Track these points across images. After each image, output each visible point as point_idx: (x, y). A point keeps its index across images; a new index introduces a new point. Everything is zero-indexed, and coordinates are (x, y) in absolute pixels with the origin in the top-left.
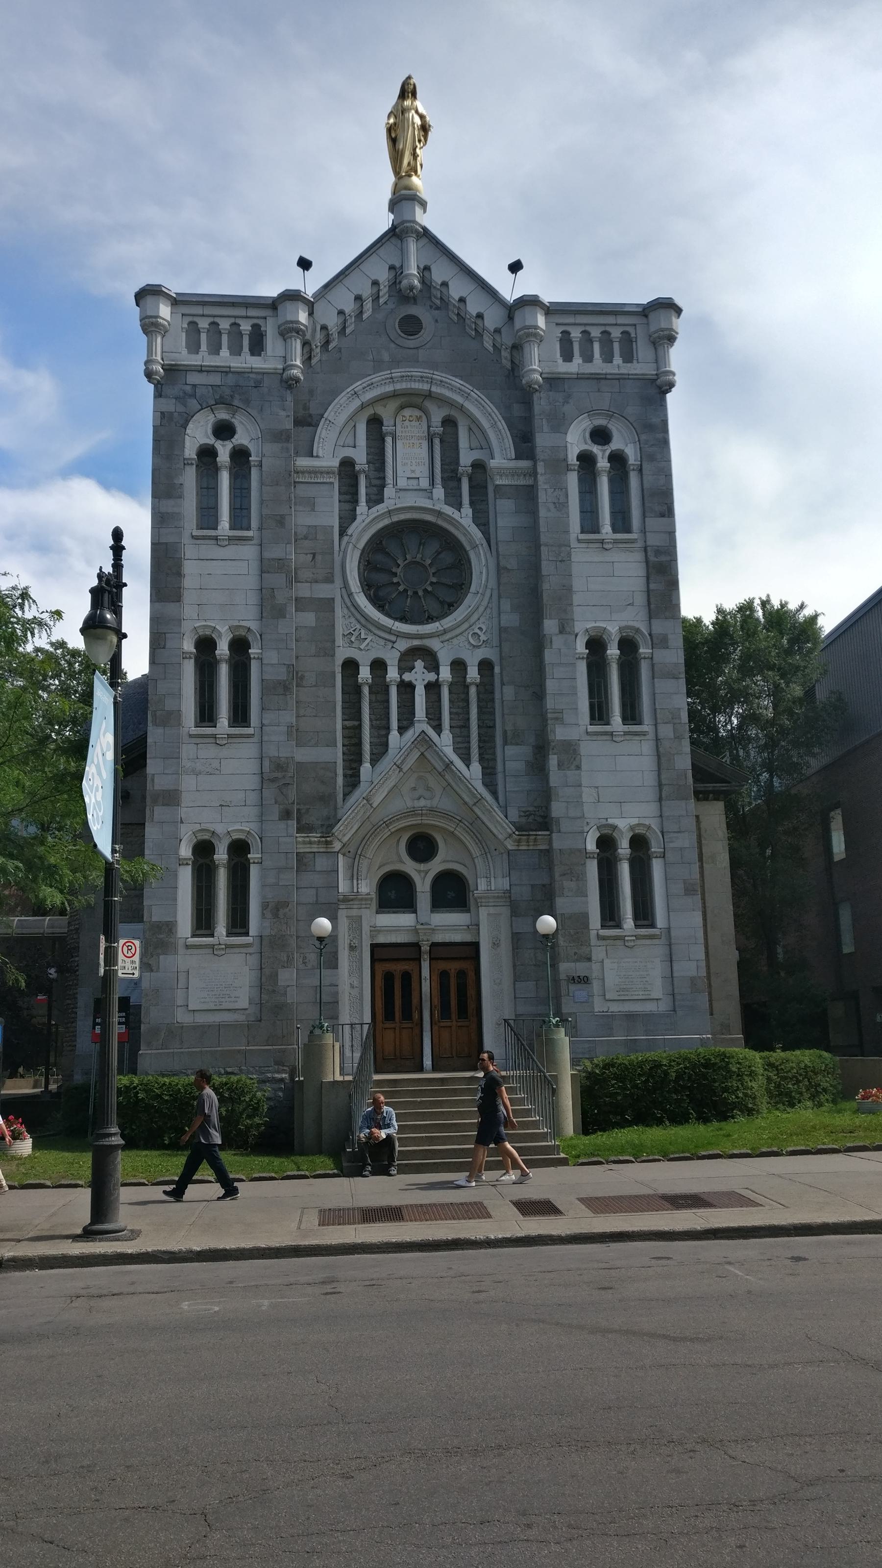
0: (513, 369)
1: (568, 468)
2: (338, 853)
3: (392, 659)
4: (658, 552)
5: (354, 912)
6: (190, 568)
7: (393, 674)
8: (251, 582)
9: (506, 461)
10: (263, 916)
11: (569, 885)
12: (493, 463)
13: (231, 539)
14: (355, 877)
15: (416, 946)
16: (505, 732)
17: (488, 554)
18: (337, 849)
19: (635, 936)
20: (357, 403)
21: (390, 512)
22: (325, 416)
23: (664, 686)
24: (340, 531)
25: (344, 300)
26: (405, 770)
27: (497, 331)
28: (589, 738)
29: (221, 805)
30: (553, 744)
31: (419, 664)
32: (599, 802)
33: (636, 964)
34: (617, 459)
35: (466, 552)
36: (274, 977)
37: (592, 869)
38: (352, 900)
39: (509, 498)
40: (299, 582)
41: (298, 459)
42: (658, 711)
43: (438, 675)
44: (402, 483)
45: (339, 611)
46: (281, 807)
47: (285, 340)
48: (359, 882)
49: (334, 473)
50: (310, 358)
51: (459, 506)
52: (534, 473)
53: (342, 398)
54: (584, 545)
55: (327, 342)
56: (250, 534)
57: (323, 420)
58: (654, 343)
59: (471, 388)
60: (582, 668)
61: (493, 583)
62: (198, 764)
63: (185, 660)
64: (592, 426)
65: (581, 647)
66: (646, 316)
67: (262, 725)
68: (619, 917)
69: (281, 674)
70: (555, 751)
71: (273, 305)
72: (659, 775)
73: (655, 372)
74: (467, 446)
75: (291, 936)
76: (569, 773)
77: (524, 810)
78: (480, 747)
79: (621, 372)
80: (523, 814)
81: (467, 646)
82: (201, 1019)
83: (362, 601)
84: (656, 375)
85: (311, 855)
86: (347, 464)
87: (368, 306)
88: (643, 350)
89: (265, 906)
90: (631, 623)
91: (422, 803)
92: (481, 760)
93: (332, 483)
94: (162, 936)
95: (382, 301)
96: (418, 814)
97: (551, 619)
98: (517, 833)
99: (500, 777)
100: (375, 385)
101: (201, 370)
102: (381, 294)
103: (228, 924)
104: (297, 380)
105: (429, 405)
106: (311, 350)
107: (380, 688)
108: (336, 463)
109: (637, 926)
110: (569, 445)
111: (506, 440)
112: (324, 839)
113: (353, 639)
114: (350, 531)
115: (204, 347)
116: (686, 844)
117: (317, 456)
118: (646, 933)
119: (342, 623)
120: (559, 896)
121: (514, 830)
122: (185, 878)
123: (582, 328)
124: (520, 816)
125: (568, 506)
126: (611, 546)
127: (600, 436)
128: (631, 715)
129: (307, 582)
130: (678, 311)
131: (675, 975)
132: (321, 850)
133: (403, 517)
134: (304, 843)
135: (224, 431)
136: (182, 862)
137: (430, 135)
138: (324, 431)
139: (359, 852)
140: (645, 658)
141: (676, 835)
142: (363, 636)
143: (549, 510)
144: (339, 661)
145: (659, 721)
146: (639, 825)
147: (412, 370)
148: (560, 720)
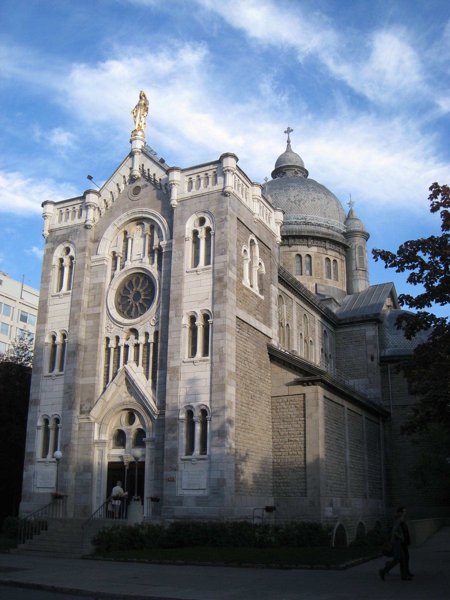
5: (101, 448)
6: (51, 309)
7: (122, 342)
11: (170, 435)
19: (196, 459)
22: (103, 237)
34: (208, 230)
44: (135, 257)
51: (153, 263)
59: (156, 212)
70: (169, 372)
73: (222, 188)
76: (174, 382)
80: (162, 402)
89: (61, 445)
101: (60, 229)
107: (118, 348)
117: (99, 254)
118: (201, 458)
122: (40, 435)
124: (161, 403)
127: (202, 221)
129: (92, 307)
138: (102, 243)
148: (172, 358)
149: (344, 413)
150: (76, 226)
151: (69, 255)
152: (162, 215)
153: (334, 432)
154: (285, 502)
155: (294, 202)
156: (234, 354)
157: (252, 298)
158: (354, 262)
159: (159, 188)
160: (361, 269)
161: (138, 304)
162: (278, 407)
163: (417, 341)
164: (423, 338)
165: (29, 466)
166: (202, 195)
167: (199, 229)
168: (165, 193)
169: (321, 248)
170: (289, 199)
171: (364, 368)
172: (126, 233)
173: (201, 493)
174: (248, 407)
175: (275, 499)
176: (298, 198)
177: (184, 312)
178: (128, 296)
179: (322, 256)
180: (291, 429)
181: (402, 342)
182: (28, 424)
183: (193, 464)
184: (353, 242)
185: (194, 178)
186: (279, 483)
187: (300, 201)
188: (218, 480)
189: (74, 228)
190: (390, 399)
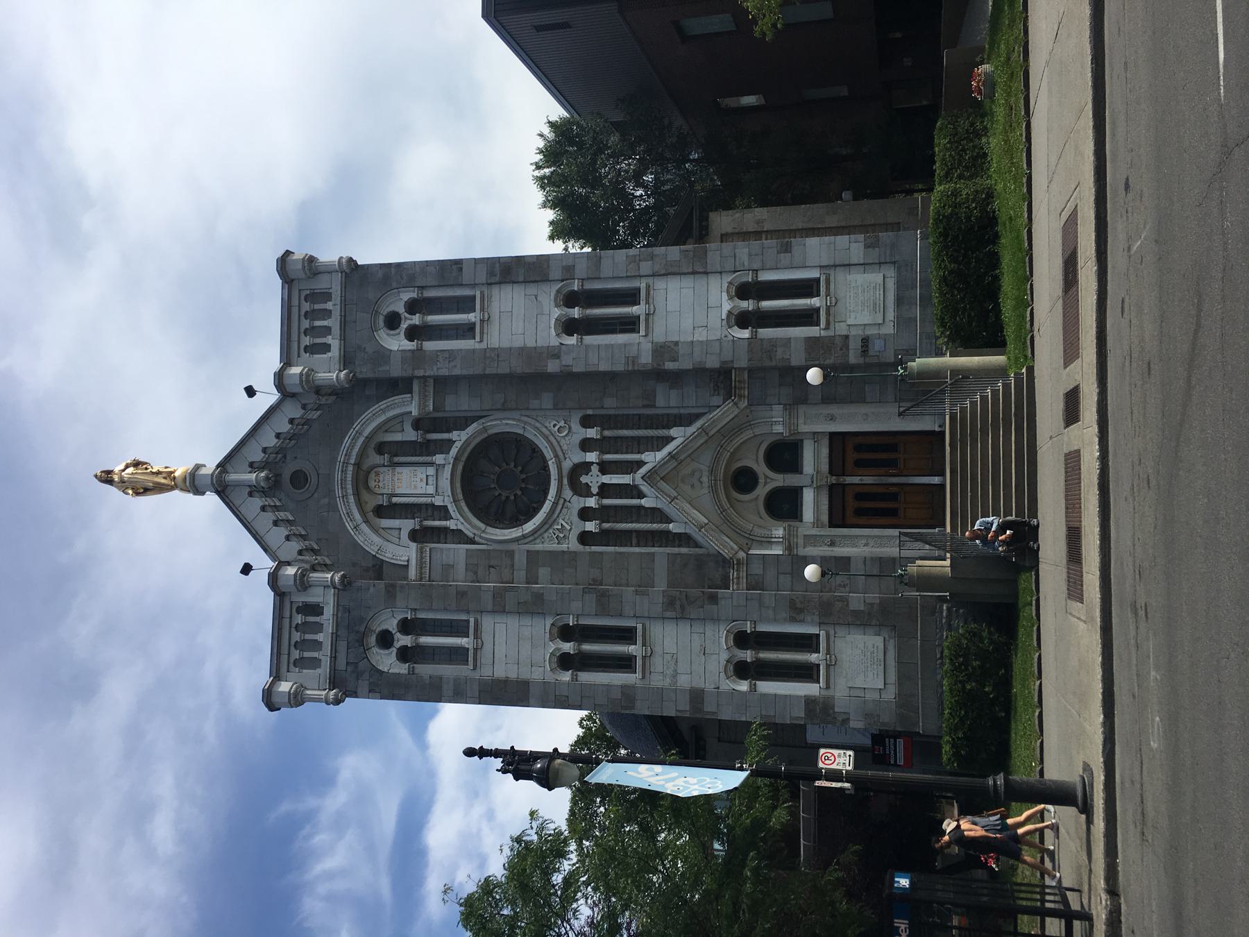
0: (337, 394)
1: (420, 349)
2: (748, 554)
3: (578, 503)
4: (491, 273)
5: (801, 541)
6: (500, 672)
7: (592, 502)
8: (513, 622)
9: (413, 402)
10: (802, 621)
11: (780, 353)
12: (415, 413)
13: (476, 637)
14: (769, 540)
15: (832, 488)
16: (645, 406)
17: (491, 418)
18: (744, 555)
19: (827, 297)
20: (364, 527)
23: (606, 270)
24: (470, 544)
26: (676, 494)
27: (304, 407)
29: (704, 654)
30: (655, 365)
31: (584, 479)
32: (707, 326)
33: (852, 297)
34: (412, 307)
35: (490, 436)
36: (856, 613)
37: (766, 333)
39: (445, 400)
40: (513, 580)
41: (410, 578)
42: (629, 274)
43: (593, 463)
44: (431, 490)
46: (706, 602)
47: (310, 586)
48: (773, 536)
49: (422, 548)
50: (326, 565)
51: (452, 442)
52: (424, 379)
53: (359, 539)
54: (485, 336)
55: (313, 550)
56: (472, 620)
57: (377, 555)
58: (315, 274)
59: (352, 430)
60: (589, 339)
61: (516, 414)
62: (668, 672)
63: (579, 679)
65: (572, 340)
66: (292, 280)
67: (635, 616)
68: (809, 310)
69: (591, 599)
70: (661, 363)
71: (280, 595)
72: (685, 274)
73: (340, 274)
74: (400, 434)
75: (820, 597)
76: (681, 352)
77: (712, 392)
78: (657, 428)
79: (339, 304)
80: (716, 393)
82: (892, 678)
83: (529, 526)
84: (342, 273)
85: (749, 578)
86: (414, 536)
87: (282, 515)
88: (321, 284)
89: (793, 620)
90: (552, 297)
91: (705, 479)
92: (669, 427)
93: (430, 549)
94: (818, 710)
96: (715, 484)
97: (546, 366)
98: (733, 398)
99: (682, 411)
100: (349, 511)
101: (334, 658)
102: (272, 504)
103: (809, 652)
104: (344, 577)
105: (365, 467)
106: (319, 564)
107: (602, 514)
108: (414, 545)
109: (818, 295)
110: (400, 348)
111: (396, 401)
112: (735, 566)
113: (562, 535)
114: (471, 535)
115: (315, 654)
116: (746, 250)
117: (408, 561)
118: (825, 286)
119: (547, 545)
120: (790, 362)
121: (731, 400)
123: (302, 335)
125: (452, 350)
127: (393, 321)
128: (631, 297)
130: (288, 253)
131: (862, 262)
132: (745, 569)
133: (459, 490)
134: (738, 584)
136: (753, 688)
137: (142, 459)
138: (387, 555)
139: (747, 536)
140: (582, 286)
141: (737, 258)
143: (455, 366)
144: (581, 548)
145: (638, 274)
146: (728, 292)
147: (336, 479)
148: (635, 359)
150: (337, 615)
151: (394, 632)
165: (836, 710)
185: (307, 341)
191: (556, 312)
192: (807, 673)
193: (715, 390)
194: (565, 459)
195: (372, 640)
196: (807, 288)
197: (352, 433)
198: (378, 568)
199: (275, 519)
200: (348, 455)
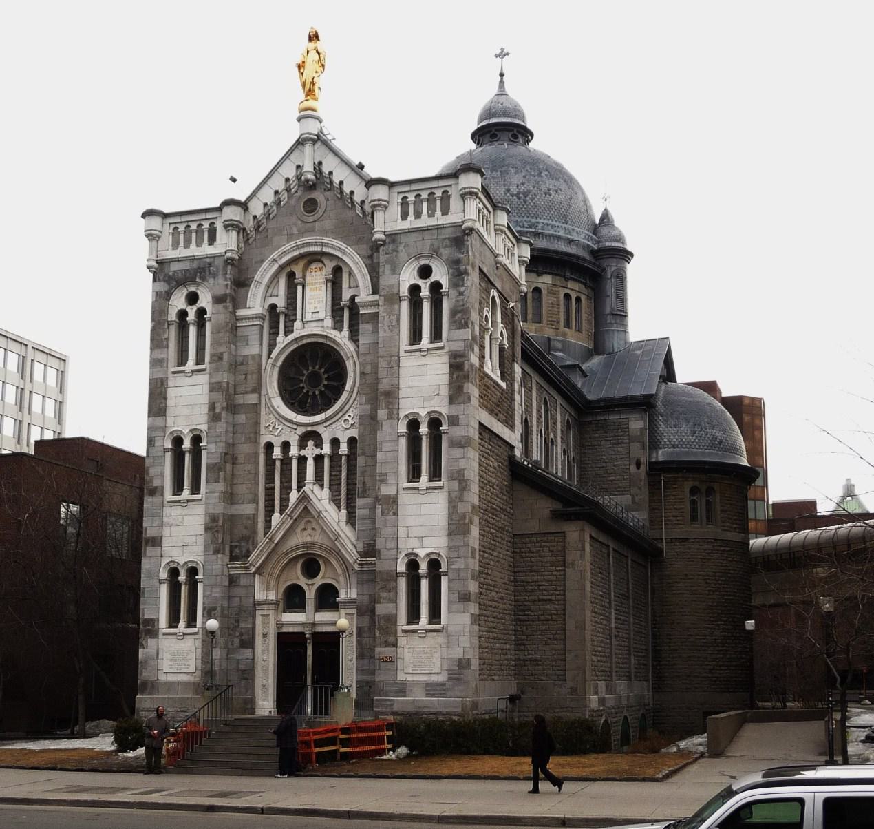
5: (265, 612)
6: (171, 393)
7: (294, 451)
11: (384, 594)
20: (276, 266)
21: (296, 340)
25: (267, 196)
28: (405, 492)
31: (311, 443)
34: (436, 287)
35: (344, 362)
37: (402, 584)
38: (264, 604)
43: (322, 449)
44: (308, 317)
45: (263, 411)
58: (463, 198)
59: (346, 246)
60: (403, 442)
64: (419, 266)
65: (403, 428)
73: (460, 221)
76: (388, 518)
81: (341, 429)
84: (462, 222)
87: (284, 197)
89: (204, 609)
91: (309, 539)
95: (293, 191)
97: (382, 409)
101: (178, 260)
104: (233, 259)
105: (324, 259)
107: (286, 461)
114: (271, 356)
117: (249, 308)
119: (265, 419)
122: (164, 591)
126: (426, 353)
127: (425, 272)
128: (435, 474)
129: (242, 393)
135: (192, 298)
141: (457, 559)
142: (277, 427)
144: (262, 444)
146: (433, 553)
148: (383, 481)
149: (609, 555)
152: (357, 253)
153: (599, 586)
154: (533, 688)
155: (516, 195)
156: (477, 478)
157: (494, 390)
158: (608, 299)
159: (350, 206)
160: (619, 313)
161: (317, 393)
162: (522, 550)
163: (707, 439)
164: (717, 434)
165: (149, 640)
166: (427, 229)
167: (420, 282)
168: (361, 215)
169: (558, 278)
170: (508, 190)
171: (624, 479)
172: (291, 275)
173: (434, 679)
174: (489, 554)
175: (518, 684)
176: (522, 189)
177: (402, 415)
178: (301, 378)
179: (559, 291)
180: (543, 583)
181: (684, 440)
182: (142, 576)
183: (420, 637)
184: (607, 266)
185: (411, 198)
186: (524, 660)
187: (526, 195)
188: (460, 660)
189: (204, 260)
190: (662, 529)
191: (423, 413)
192: (174, 620)
193: (367, 544)
194: (326, 427)
195: (192, 289)
196: (435, 615)
197: (343, 246)
198: (241, 283)
199: (279, 191)
200: (328, 245)
